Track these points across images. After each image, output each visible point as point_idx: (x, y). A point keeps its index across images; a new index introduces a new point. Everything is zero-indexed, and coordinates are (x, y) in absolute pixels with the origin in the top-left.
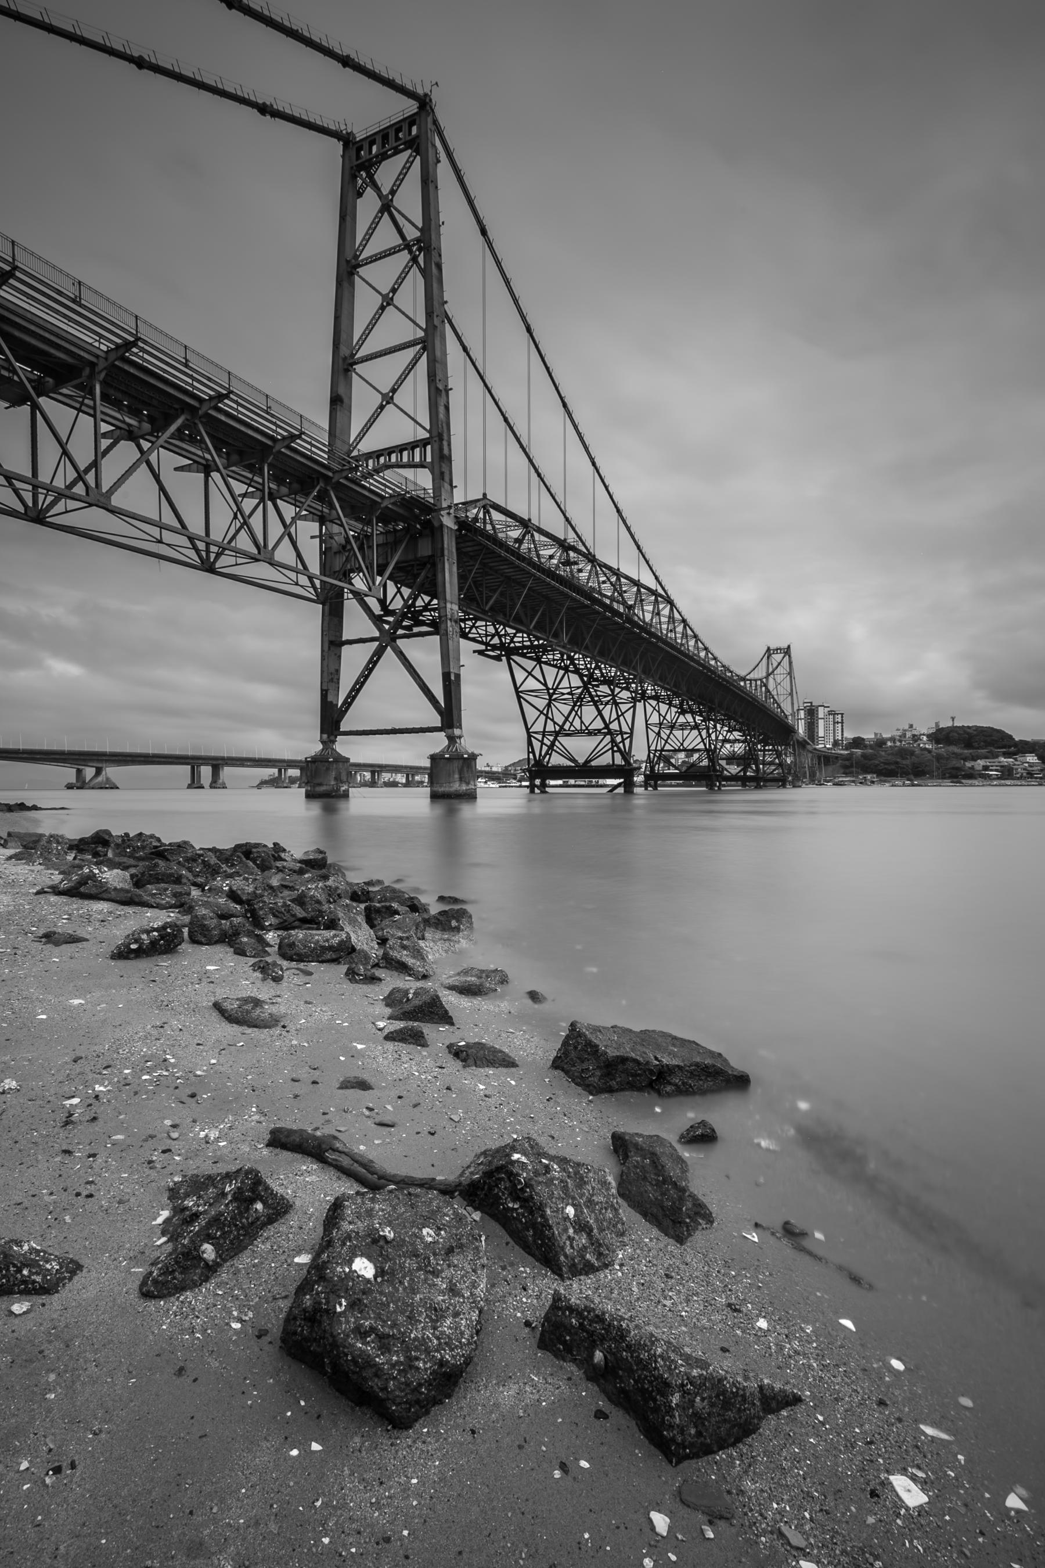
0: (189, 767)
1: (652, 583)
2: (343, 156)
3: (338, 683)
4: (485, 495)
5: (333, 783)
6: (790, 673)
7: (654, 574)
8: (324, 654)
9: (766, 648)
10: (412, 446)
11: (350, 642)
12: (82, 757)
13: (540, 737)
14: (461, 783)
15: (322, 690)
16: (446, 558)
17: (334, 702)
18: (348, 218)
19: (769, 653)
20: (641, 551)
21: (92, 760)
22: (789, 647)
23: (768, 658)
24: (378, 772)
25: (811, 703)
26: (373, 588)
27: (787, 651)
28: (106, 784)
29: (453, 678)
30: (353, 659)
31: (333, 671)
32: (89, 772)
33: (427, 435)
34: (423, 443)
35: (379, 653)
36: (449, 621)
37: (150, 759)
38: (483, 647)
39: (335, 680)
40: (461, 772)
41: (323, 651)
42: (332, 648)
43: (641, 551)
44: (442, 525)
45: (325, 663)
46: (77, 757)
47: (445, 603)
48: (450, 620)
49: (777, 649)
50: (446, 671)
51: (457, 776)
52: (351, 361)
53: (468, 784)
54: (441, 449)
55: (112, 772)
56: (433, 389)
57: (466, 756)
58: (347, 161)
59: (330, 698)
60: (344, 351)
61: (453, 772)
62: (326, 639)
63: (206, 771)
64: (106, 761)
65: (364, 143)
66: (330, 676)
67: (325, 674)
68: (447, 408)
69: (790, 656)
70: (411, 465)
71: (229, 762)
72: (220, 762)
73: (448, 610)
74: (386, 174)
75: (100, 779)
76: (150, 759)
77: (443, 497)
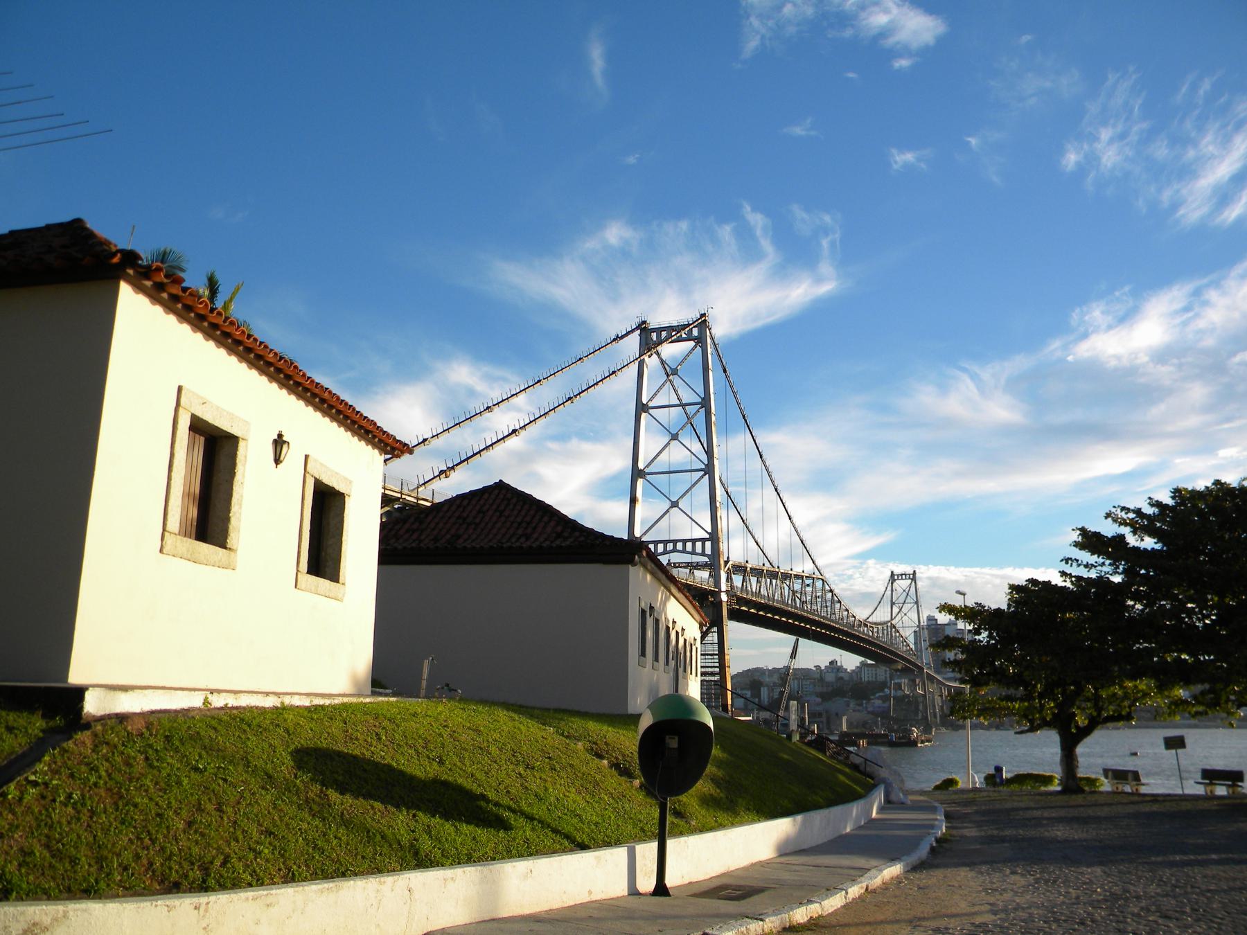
1: (808, 568)
6: (917, 602)
7: (812, 560)
9: (890, 573)
10: (694, 541)
19: (893, 578)
20: (804, 545)
22: (914, 571)
23: (892, 584)
25: (937, 620)
27: (913, 576)
33: (708, 536)
34: (703, 540)
43: (804, 545)
44: (721, 602)
49: (902, 575)
65: (656, 330)
68: (721, 517)
69: (915, 583)
70: (693, 552)
74: (670, 350)
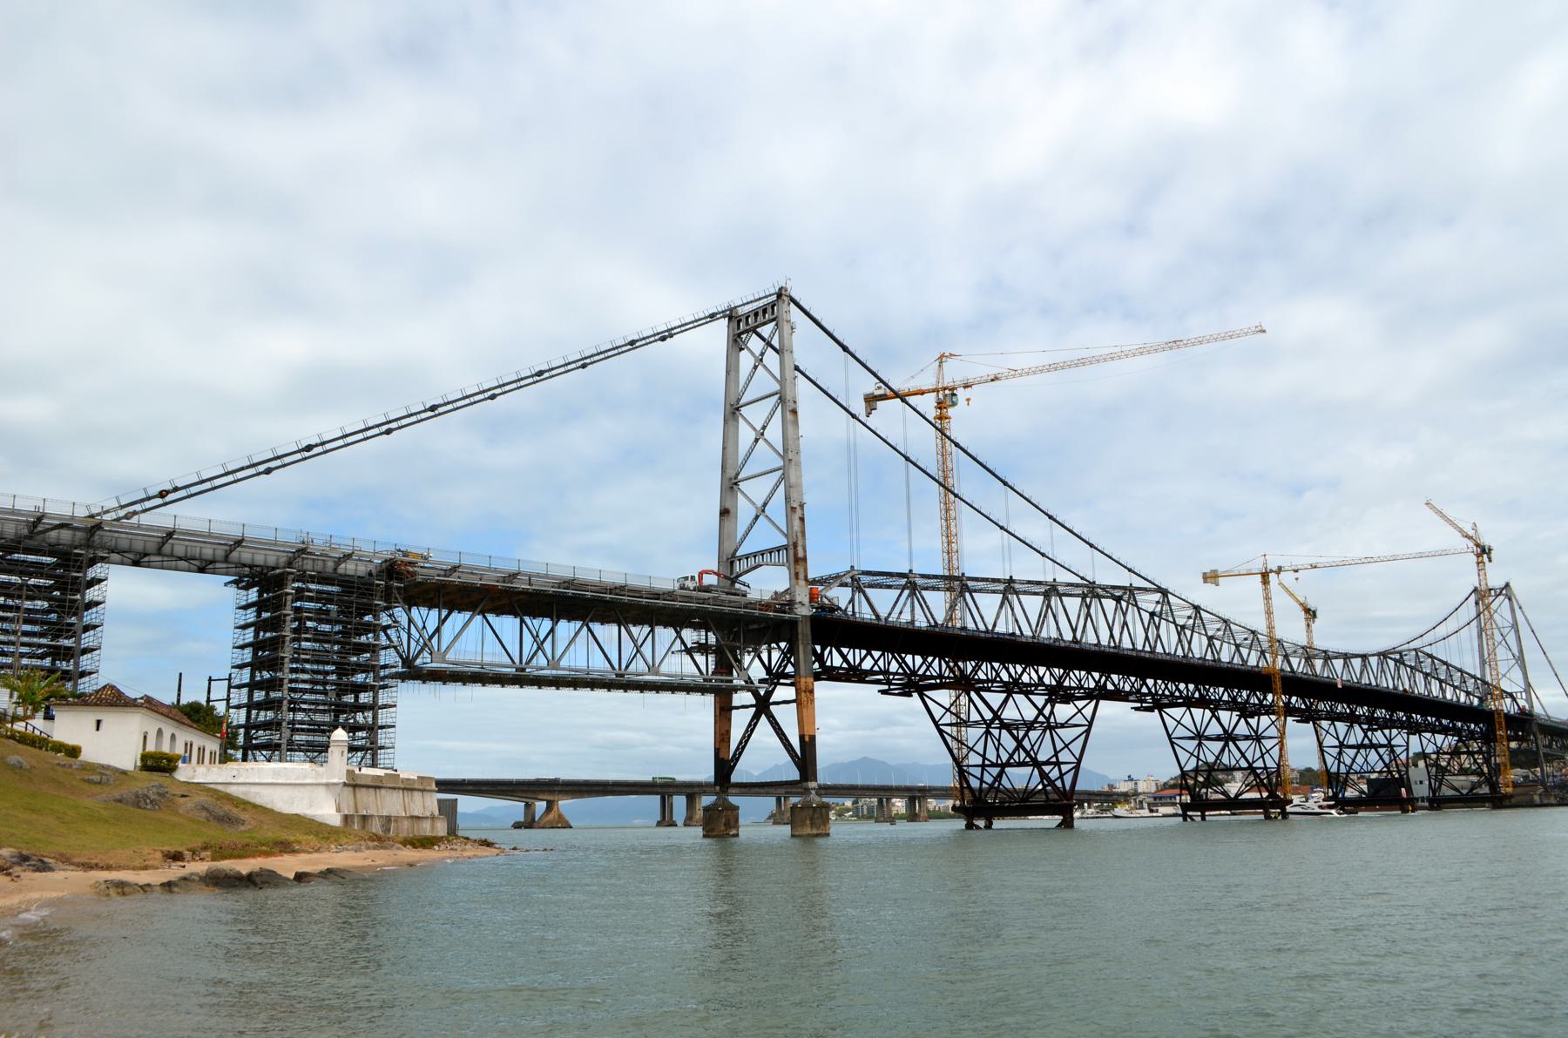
0: (659, 797)
2: (728, 327)
3: (729, 742)
4: (852, 567)
5: (723, 828)
11: (737, 708)
13: (977, 772)
14: (812, 828)
16: (800, 642)
17: (726, 758)
18: (732, 373)
21: (543, 792)
24: (919, 797)
26: (740, 673)
28: (558, 823)
30: (740, 720)
31: (724, 731)
32: (540, 806)
35: (756, 717)
36: (803, 693)
38: (886, 687)
39: (726, 740)
40: (812, 819)
42: (722, 713)
45: (718, 725)
46: (526, 788)
48: (805, 692)
51: (808, 822)
52: (736, 481)
54: (796, 554)
55: (566, 805)
56: (789, 509)
57: (814, 805)
58: (731, 329)
60: (731, 473)
61: (806, 819)
62: (718, 705)
63: (679, 802)
64: (560, 792)
66: (722, 735)
67: (718, 736)
72: (696, 790)
75: (551, 816)
76: (610, 788)
77: (797, 593)
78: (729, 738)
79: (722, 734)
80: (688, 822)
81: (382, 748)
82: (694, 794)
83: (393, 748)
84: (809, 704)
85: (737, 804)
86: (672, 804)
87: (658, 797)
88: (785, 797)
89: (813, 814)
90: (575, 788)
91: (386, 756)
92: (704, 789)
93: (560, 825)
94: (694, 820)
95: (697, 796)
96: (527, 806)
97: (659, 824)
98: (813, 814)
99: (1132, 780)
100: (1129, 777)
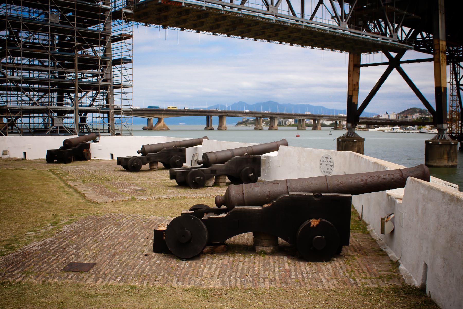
0: (206, 116)
3: (358, 91)
8: (350, 73)
11: (367, 65)
12: (152, 112)
14: (448, 161)
15: (348, 96)
16: (439, 11)
17: (356, 103)
21: (156, 114)
24: (318, 119)
28: (164, 127)
29: (443, 91)
31: (355, 83)
32: (154, 121)
37: (186, 113)
39: (356, 89)
40: (448, 154)
41: (349, 71)
42: (355, 69)
45: (351, 78)
46: (149, 112)
47: (439, 41)
48: (442, 52)
50: (438, 85)
51: (446, 156)
53: (453, 161)
55: (166, 120)
59: (354, 101)
61: (444, 154)
62: (352, 64)
63: (215, 119)
64: (164, 114)
67: (351, 86)
71: (229, 114)
72: (223, 114)
73: (441, 46)
75: (160, 125)
76: (186, 113)
78: (358, 88)
79: (355, 85)
80: (220, 128)
81: (118, 86)
82: (223, 116)
83: (131, 86)
84: (444, 62)
85: (363, 137)
86: (212, 120)
87: (205, 117)
88: (260, 118)
89: (450, 150)
90: (171, 112)
91: (124, 96)
92: (227, 114)
93: (164, 129)
94: (223, 127)
95: (224, 117)
96: (149, 120)
97: (206, 128)
98: (450, 150)
99: (387, 114)
100: (386, 112)
